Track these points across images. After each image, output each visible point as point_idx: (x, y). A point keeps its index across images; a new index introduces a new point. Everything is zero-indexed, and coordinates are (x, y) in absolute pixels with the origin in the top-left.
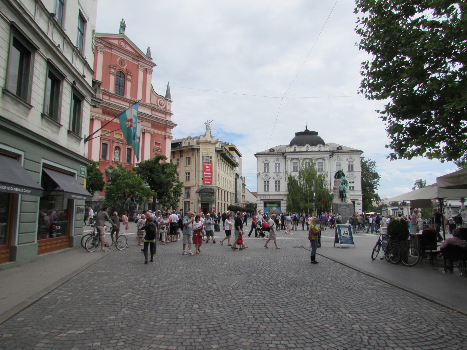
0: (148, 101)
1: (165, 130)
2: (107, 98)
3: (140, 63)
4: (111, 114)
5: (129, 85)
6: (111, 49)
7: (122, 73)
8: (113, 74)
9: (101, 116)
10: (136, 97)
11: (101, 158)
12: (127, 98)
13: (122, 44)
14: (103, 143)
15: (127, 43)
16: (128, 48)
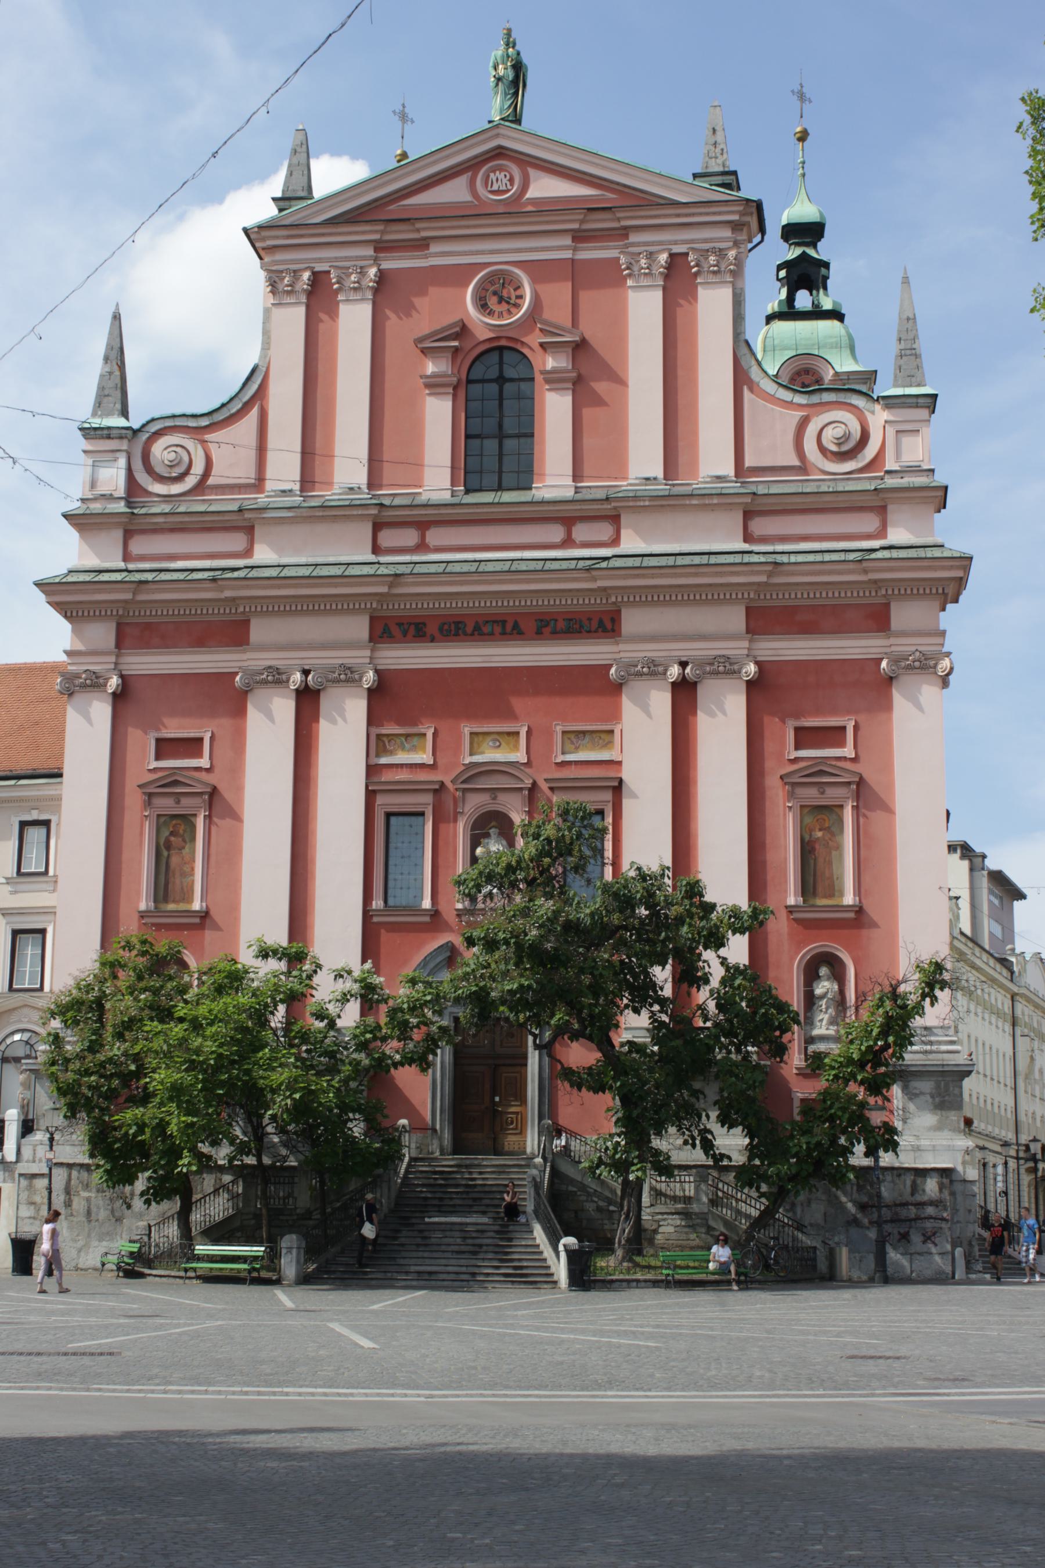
0: (713, 459)
1: (878, 619)
2: (409, 537)
3: (634, 238)
4: (432, 629)
5: (555, 410)
6: (422, 245)
7: (507, 355)
8: (434, 385)
9: (359, 657)
10: (620, 469)
11: (377, 903)
12: (548, 494)
13: (499, 180)
14: (388, 815)
15: (527, 162)
16: (545, 187)
